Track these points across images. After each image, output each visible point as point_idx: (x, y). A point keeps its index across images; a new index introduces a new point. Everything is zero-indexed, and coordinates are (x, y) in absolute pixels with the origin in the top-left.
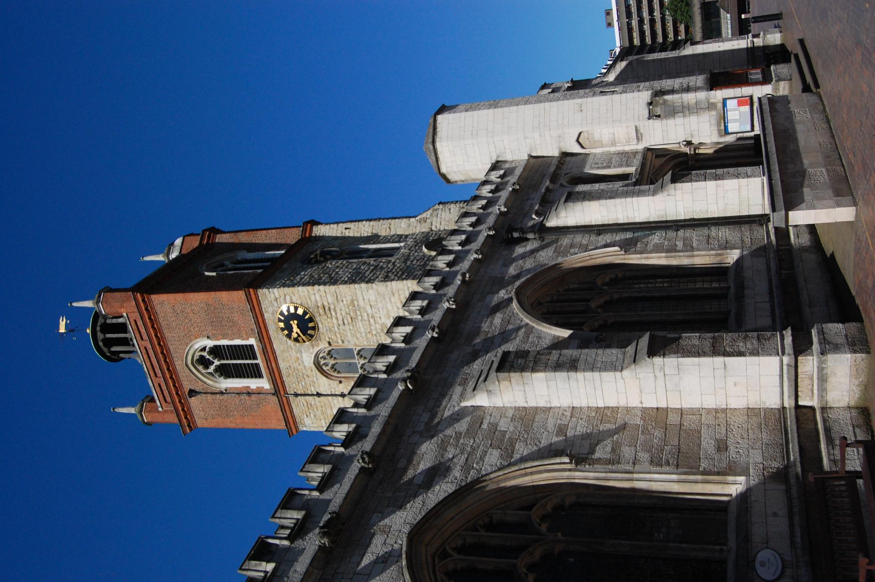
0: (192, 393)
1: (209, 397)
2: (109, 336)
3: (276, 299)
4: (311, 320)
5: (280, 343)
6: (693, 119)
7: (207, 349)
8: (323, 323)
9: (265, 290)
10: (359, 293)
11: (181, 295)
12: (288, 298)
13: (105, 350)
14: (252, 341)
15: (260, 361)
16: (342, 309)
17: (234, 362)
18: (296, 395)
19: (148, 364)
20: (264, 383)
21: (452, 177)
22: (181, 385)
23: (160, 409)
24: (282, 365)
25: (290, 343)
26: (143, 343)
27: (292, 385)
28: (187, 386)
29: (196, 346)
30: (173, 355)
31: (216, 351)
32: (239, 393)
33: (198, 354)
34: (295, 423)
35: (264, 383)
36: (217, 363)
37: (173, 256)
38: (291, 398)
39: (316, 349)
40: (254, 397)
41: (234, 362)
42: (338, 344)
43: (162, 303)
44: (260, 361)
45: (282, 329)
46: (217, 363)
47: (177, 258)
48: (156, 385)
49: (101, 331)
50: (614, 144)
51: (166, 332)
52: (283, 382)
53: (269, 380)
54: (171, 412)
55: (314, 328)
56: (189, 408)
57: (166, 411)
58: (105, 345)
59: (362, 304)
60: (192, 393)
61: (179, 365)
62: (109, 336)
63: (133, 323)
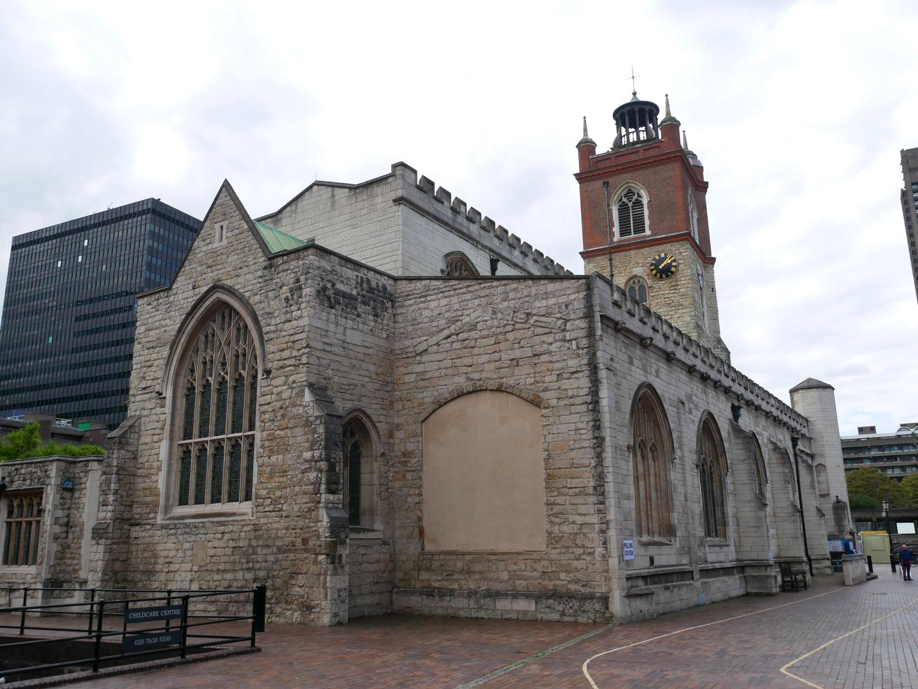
0: (606, 184)
2: (637, 115)
3: (681, 253)
4: (667, 276)
5: (649, 255)
6: (833, 524)
8: (664, 285)
10: (688, 310)
12: (682, 261)
13: (626, 110)
14: (648, 232)
15: (633, 236)
16: (676, 298)
17: (630, 218)
18: (611, 260)
22: (612, 176)
24: (633, 253)
25: (650, 259)
26: (641, 151)
27: (618, 258)
28: (611, 180)
31: (638, 203)
34: (589, 257)
35: (617, 238)
36: (630, 204)
37: (690, 160)
38: (608, 256)
39: (646, 277)
41: (630, 218)
42: (650, 294)
44: (633, 236)
45: (659, 256)
46: (630, 204)
47: (689, 163)
49: (640, 109)
50: (819, 483)
52: (620, 251)
53: (620, 241)
55: (661, 277)
56: (594, 180)
59: (680, 311)
60: (606, 184)
61: (626, 176)
62: (637, 115)
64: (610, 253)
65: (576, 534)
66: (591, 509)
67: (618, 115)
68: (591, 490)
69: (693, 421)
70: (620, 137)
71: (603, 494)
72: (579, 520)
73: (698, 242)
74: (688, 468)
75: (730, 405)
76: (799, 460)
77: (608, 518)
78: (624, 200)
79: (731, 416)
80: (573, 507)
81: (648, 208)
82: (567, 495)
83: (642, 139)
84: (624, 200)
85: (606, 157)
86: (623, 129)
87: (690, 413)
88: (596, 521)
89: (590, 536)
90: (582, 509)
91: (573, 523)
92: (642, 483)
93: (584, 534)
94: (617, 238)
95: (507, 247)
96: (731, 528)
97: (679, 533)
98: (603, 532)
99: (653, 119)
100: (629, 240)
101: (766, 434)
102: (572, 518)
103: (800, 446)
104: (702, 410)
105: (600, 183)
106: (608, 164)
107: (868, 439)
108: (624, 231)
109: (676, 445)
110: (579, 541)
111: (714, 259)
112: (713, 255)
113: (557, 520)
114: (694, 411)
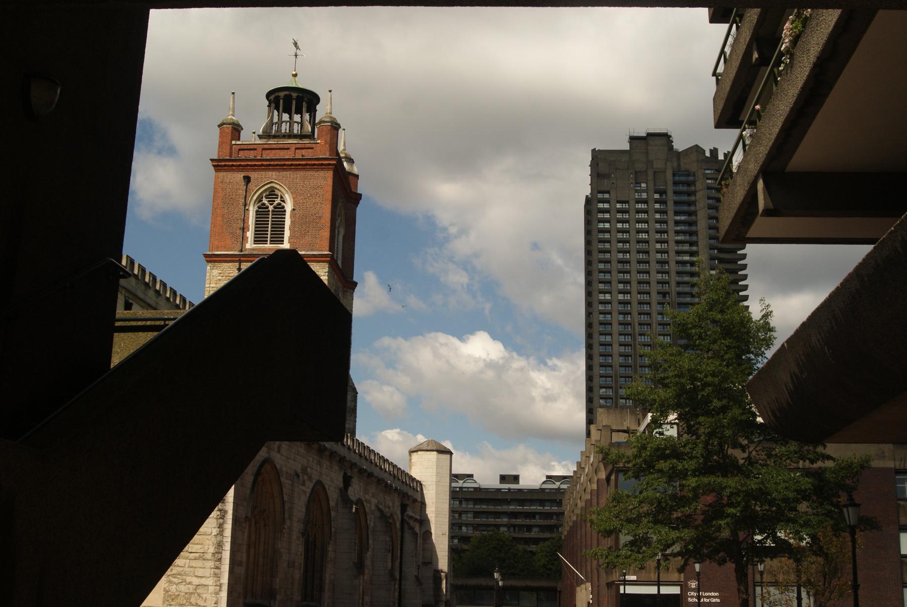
0: (247, 180)
1: (243, 193)
2: (294, 102)
7: (283, 204)
9: (327, 269)
11: (330, 197)
13: (282, 94)
19: (274, 146)
20: (250, 245)
21: (414, 455)
22: (255, 170)
23: (233, 142)
28: (253, 175)
29: (287, 196)
30: (282, 173)
32: (245, 221)
33: (279, 194)
34: (215, 261)
36: (271, 208)
37: (345, 164)
38: (237, 264)
40: (240, 232)
43: (325, 178)
46: (271, 208)
48: (255, 147)
51: (301, 174)
53: (253, 250)
54: (231, 153)
56: (233, 171)
57: (231, 148)
58: (286, 96)
60: (247, 180)
61: (272, 175)
62: (294, 102)
63: (310, 146)
64: (240, 262)
65: (192, 593)
66: (208, 572)
67: (272, 97)
68: (209, 556)
69: (305, 493)
70: (271, 123)
71: (220, 560)
72: (196, 581)
73: (340, 263)
74: (294, 537)
75: (342, 474)
76: (406, 526)
77: (222, 581)
78: (265, 201)
79: (341, 485)
80: (192, 569)
81: (293, 215)
82: (187, 558)
83: (295, 132)
84: (265, 201)
85: (251, 148)
86: (276, 113)
87: (304, 484)
88: (211, 583)
89: (204, 596)
90: (200, 572)
91: (190, 583)
92: (252, 551)
93: (199, 595)
94: (250, 245)
95: (143, 287)
96: (327, 595)
97: (278, 597)
98: (217, 593)
99: (312, 111)
100: (264, 250)
101: (374, 501)
102: (188, 579)
103: (410, 512)
104: (314, 481)
105: (239, 176)
106: (251, 155)
107: (509, 489)
108: (259, 238)
109: (287, 516)
110: (193, 600)
111: (356, 284)
112: (355, 279)
113: (175, 580)
114: (307, 483)
